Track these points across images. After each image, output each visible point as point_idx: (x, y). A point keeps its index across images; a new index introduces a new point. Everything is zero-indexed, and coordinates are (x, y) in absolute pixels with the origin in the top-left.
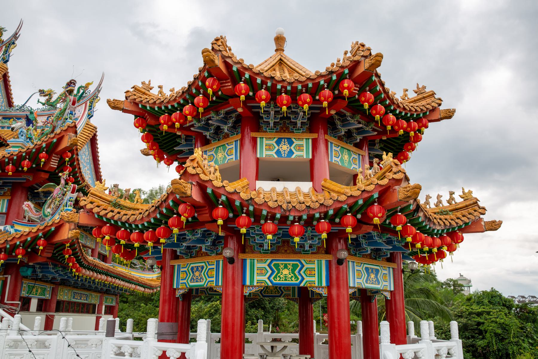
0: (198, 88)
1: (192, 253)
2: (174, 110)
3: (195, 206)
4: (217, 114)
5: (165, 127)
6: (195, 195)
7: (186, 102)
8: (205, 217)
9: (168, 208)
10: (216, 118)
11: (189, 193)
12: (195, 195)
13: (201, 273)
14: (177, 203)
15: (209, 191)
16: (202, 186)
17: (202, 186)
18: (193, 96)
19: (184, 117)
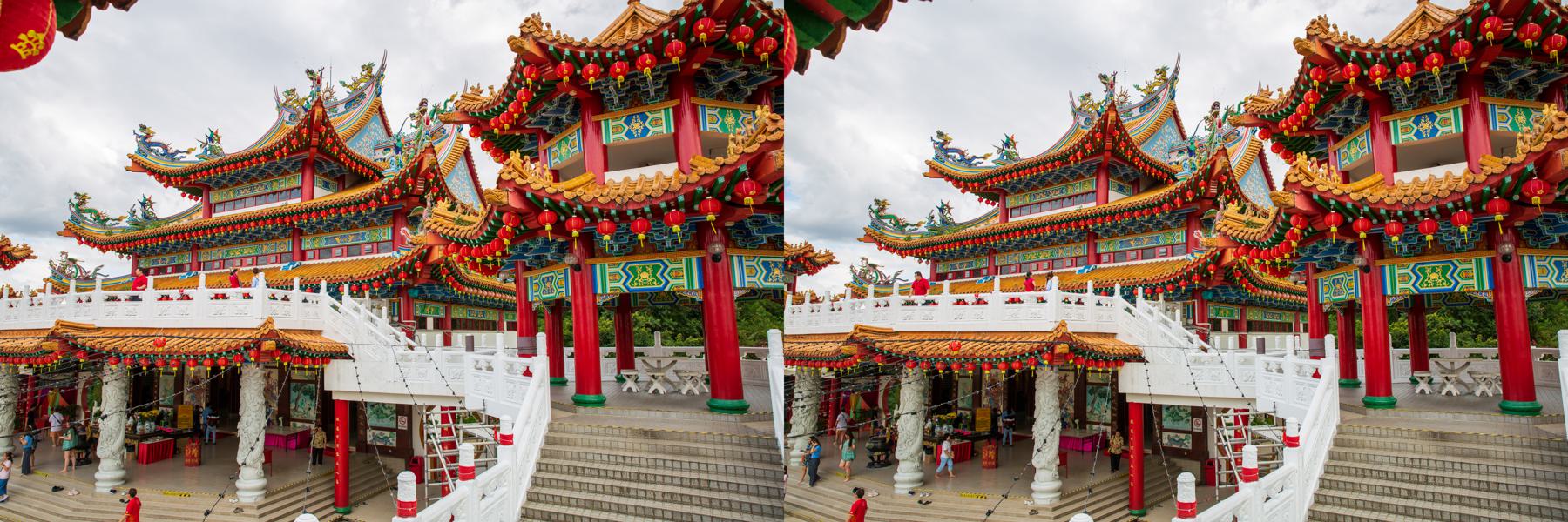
0: (519, 82)
1: (540, 263)
2: (501, 110)
3: (518, 213)
4: (551, 102)
5: (496, 131)
6: (514, 202)
7: (511, 98)
8: (532, 225)
9: (495, 219)
10: (550, 108)
11: (505, 201)
12: (514, 202)
13: (549, 285)
14: (501, 213)
15: (529, 195)
16: (520, 191)
17: (520, 191)
18: (515, 91)
19: (510, 115)
